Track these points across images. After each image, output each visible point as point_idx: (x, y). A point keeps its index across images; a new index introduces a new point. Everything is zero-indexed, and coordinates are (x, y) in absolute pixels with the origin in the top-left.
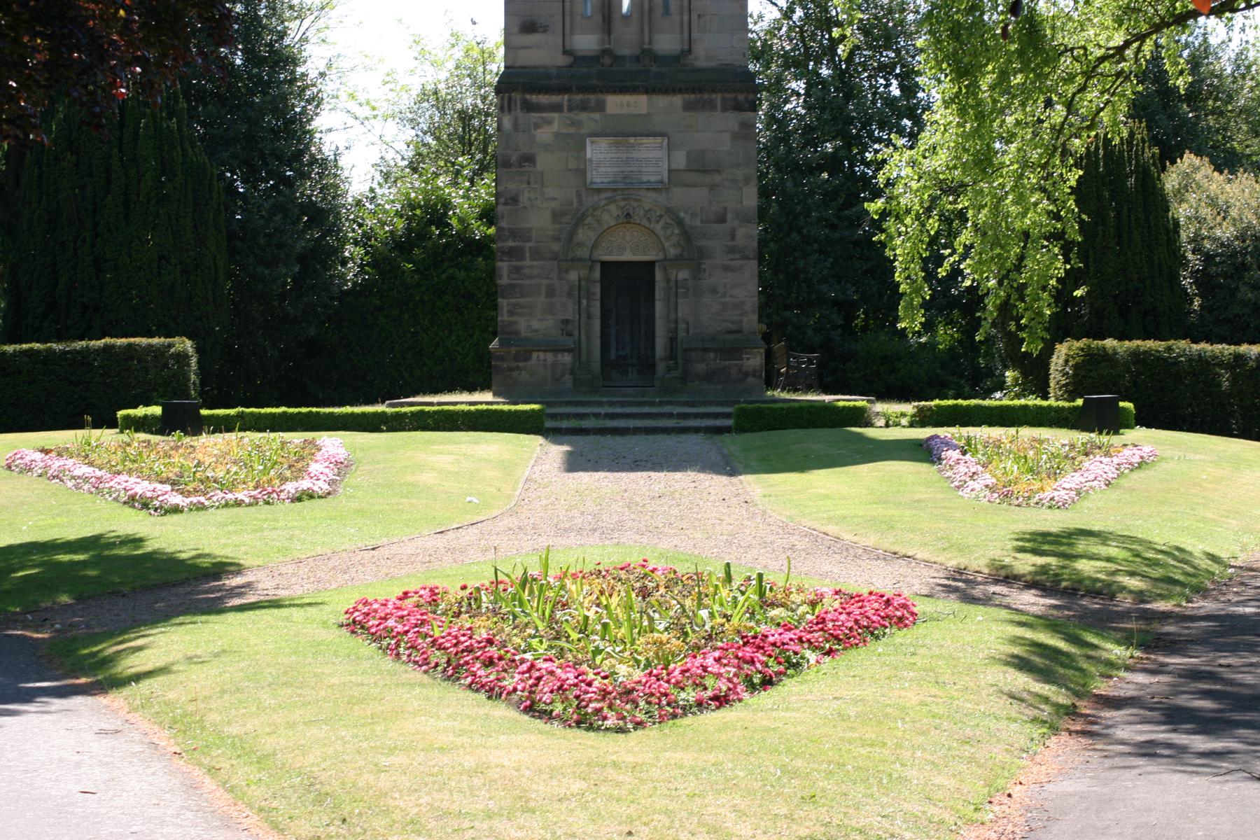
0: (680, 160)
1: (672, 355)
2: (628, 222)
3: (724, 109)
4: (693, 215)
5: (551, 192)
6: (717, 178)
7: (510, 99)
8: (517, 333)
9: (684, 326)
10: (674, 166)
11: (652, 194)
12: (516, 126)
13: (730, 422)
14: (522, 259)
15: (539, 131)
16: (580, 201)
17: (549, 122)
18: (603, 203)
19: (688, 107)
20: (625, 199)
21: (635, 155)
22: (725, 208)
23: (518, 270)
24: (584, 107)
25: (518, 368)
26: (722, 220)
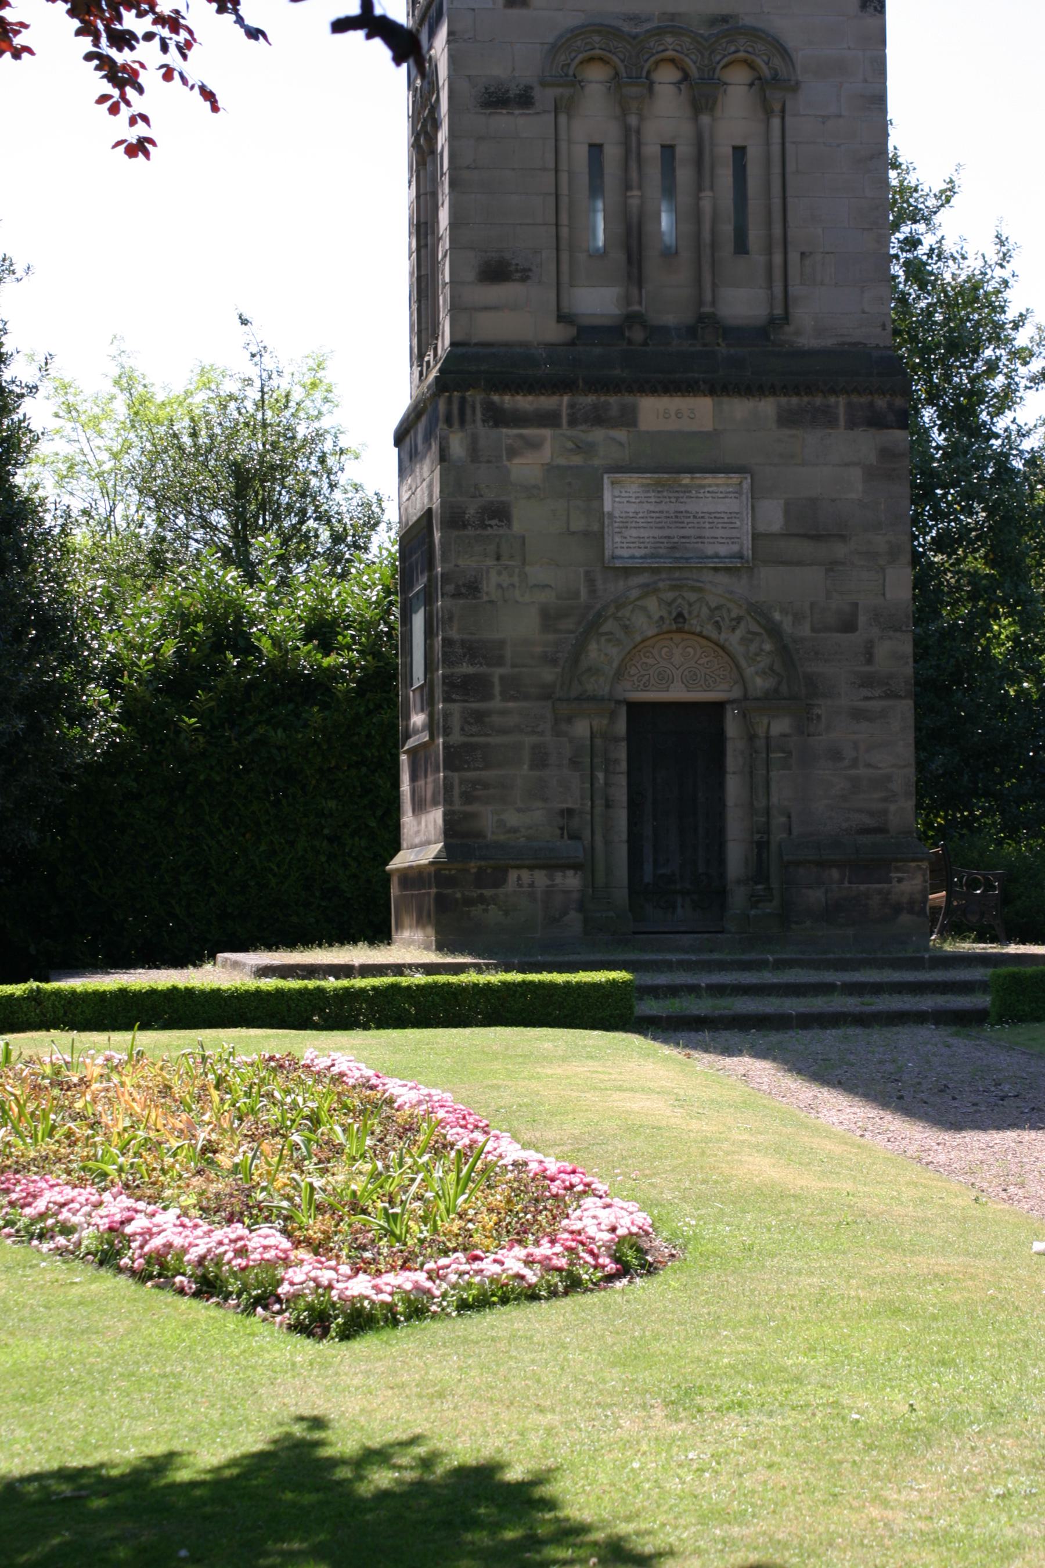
0: (773, 516)
2: (680, 631)
3: (851, 425)
5: (537, 573)
6: (840, 550)
7: (463, 401)
8: (480, 834)
9: (783, 819)
10: (762, 528)
11: (723, 579)
12: (474, 452)
13: (983, 1001)
14: (488, 697)
15: (516, 461)
16: (593, 592)
17: (534, 445)
18: (634, 594)
19: (787, 419)
20: (673, 588)
21: (692, 506)
22: (856, 604)
23: (479, 717)
24: (598, 418)
25: (482, 899)
26: (849, 625)
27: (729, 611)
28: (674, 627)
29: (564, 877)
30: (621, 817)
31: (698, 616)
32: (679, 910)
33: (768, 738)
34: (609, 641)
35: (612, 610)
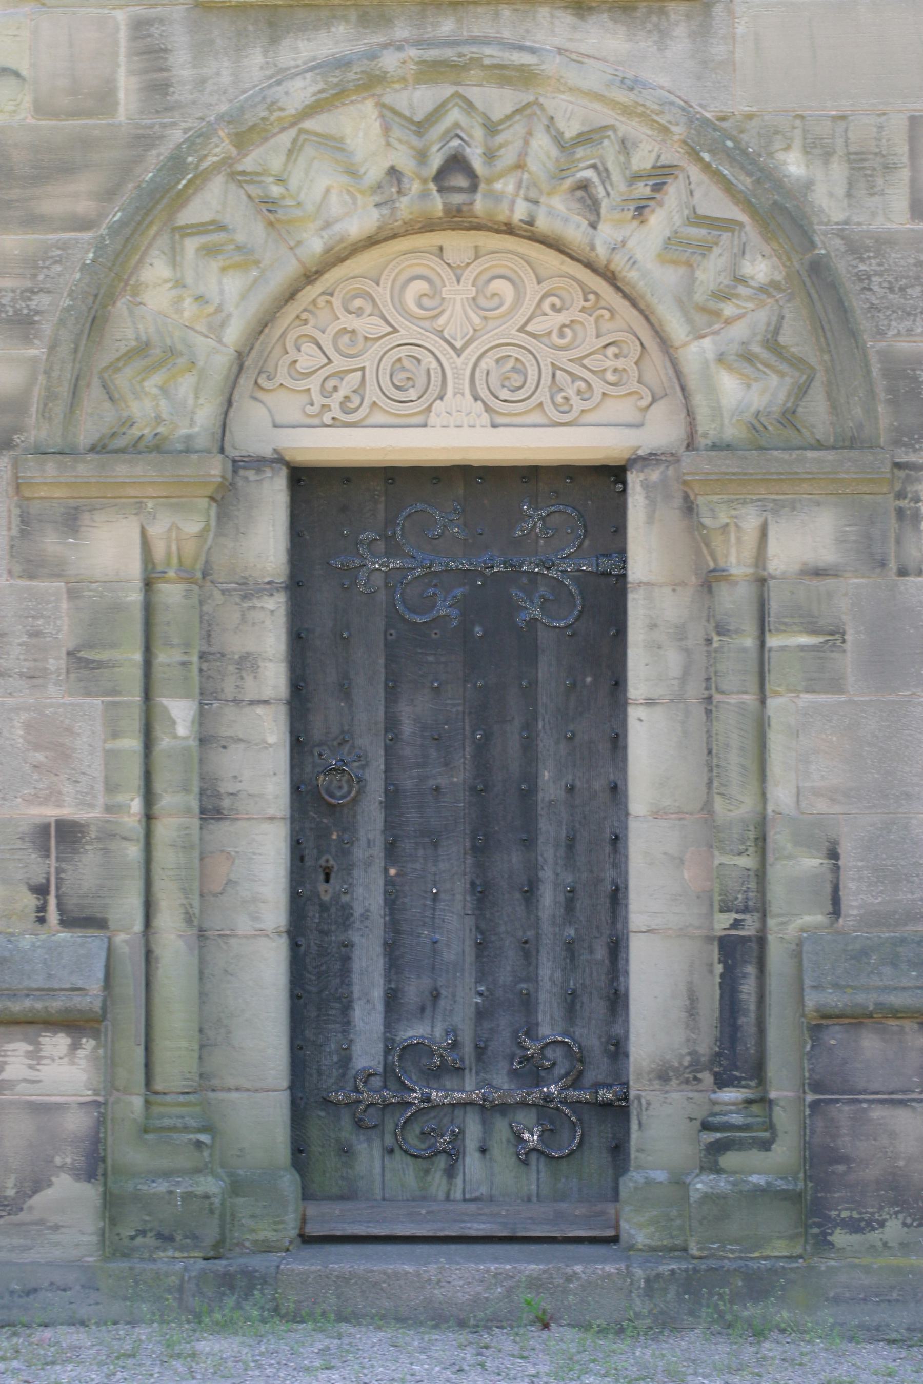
1: (734, 1055)
2: (458, 220)
4: (865, 169)
9: (812, 863)
16: (157, 89)
18: (300, 92)
20: (432, 71)
27: (625, 146)
28: (437, 204)
29: (36, 1056)
30: (263, 856)
31: (520, 166)
32: (472, 1162)
33: (762, 582)
34: (210, 251)
35: (221, 147)
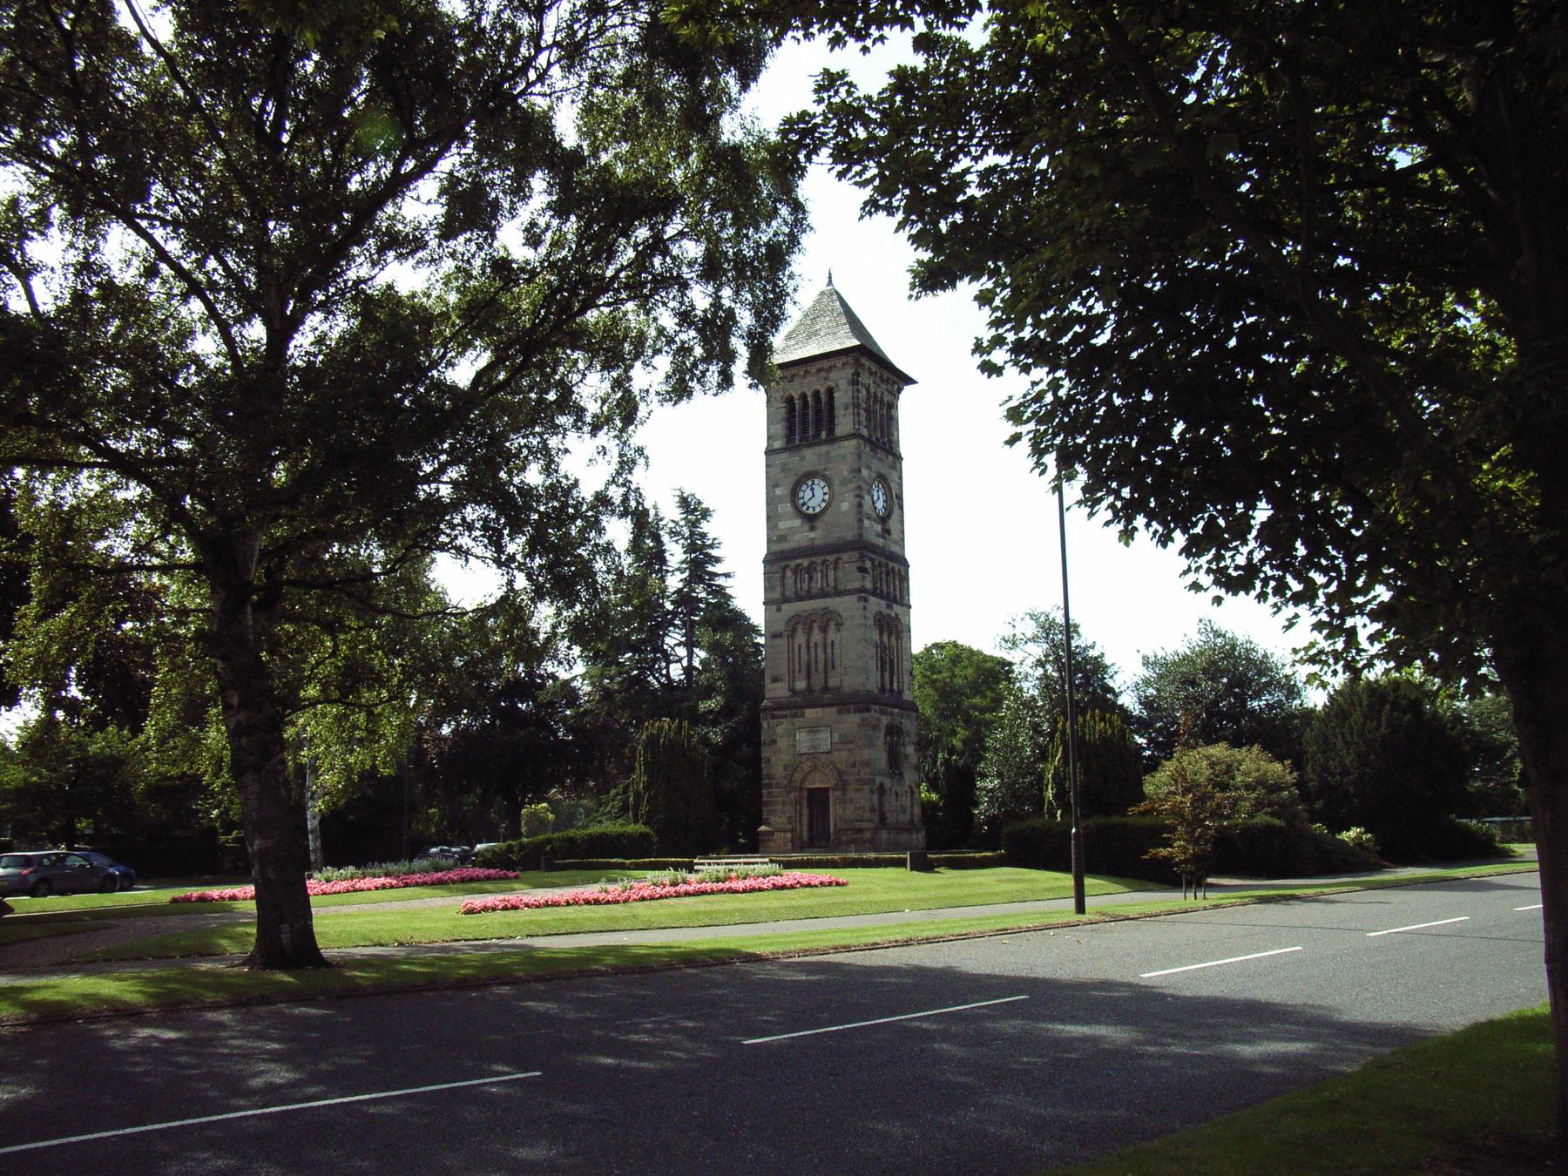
19: (839, 712)
24: (795, 716)
